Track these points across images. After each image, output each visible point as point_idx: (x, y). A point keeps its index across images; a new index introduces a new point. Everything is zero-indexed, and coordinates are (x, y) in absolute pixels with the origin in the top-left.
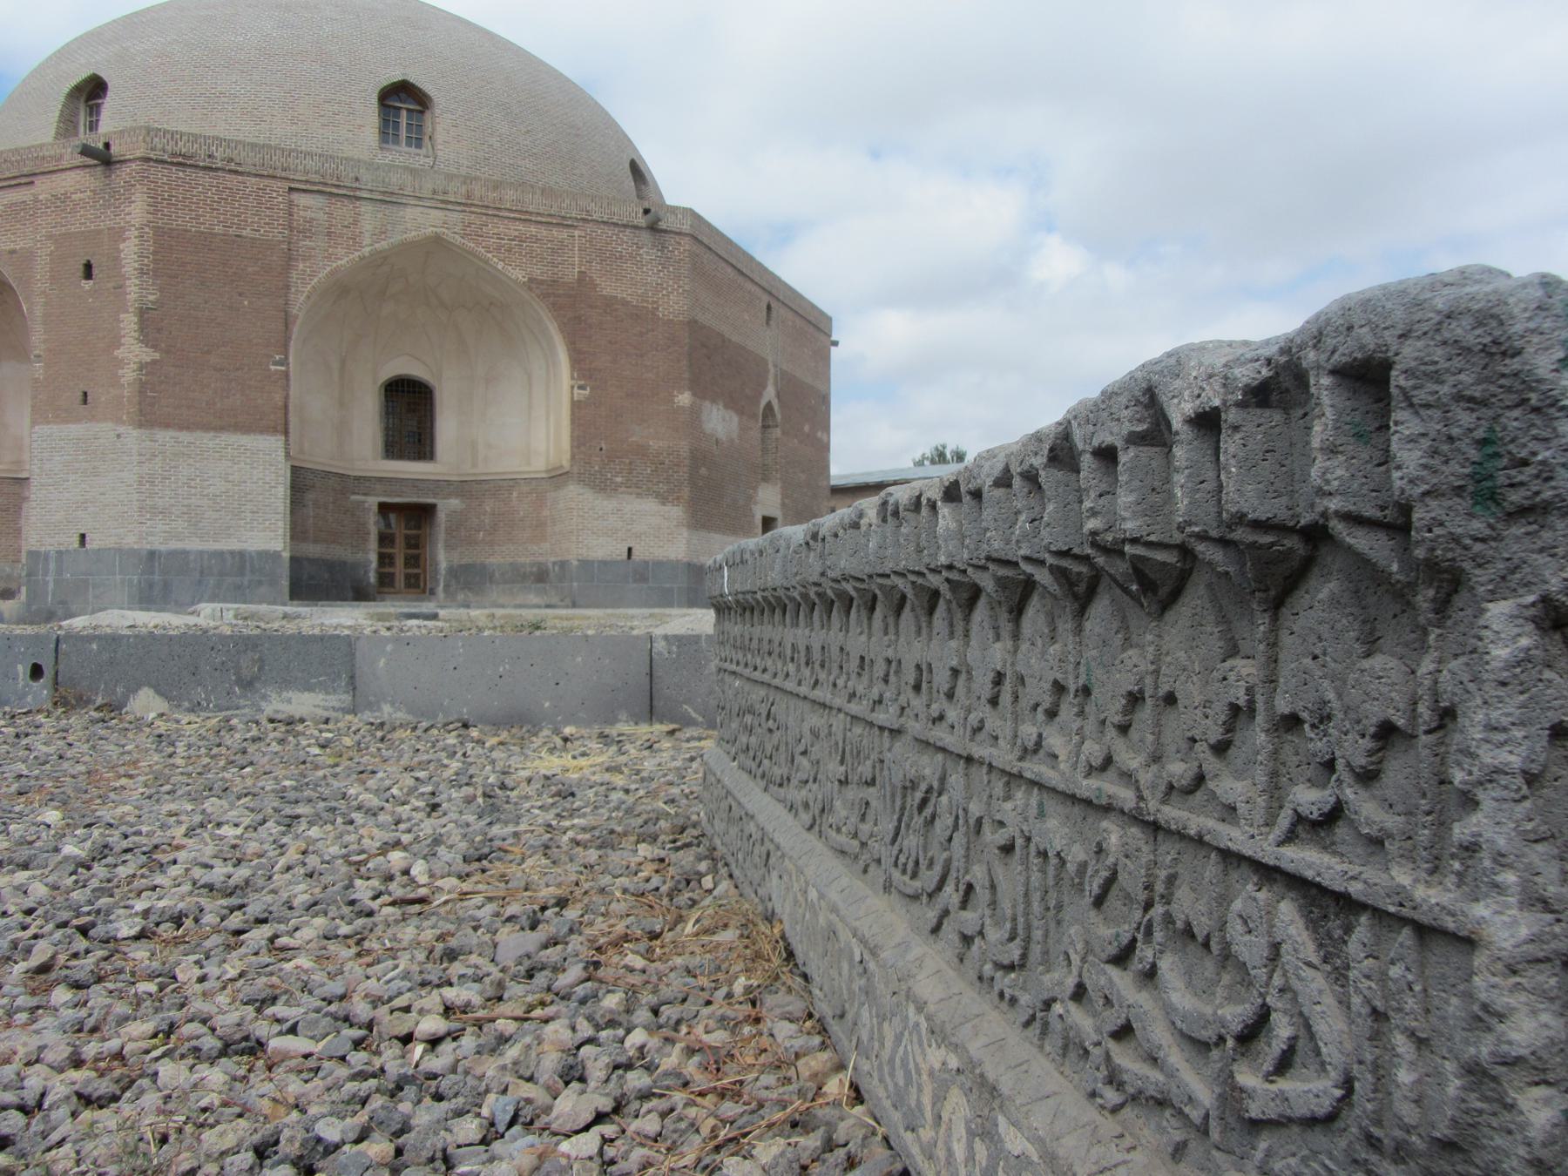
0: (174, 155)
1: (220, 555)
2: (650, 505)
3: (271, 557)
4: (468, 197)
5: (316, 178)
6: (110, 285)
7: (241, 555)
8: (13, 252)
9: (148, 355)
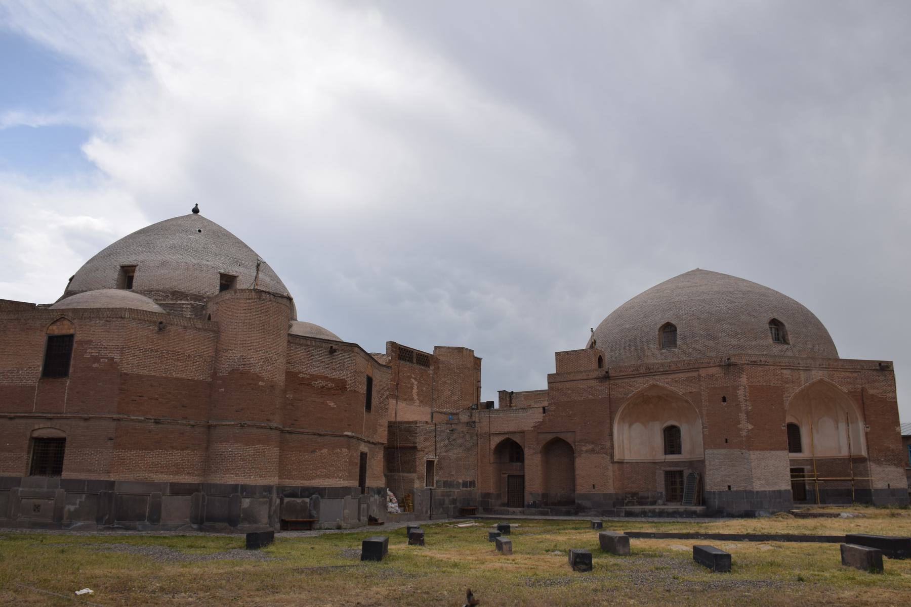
0: (751, 362)
1: (774, 491)
2: (892, 469)
3: (786, 491)
4: (829, 365)
5: (787, 364)
6: (734, 404)
7: (780, 492)
8: (691, 393)
9: (750, 427)
